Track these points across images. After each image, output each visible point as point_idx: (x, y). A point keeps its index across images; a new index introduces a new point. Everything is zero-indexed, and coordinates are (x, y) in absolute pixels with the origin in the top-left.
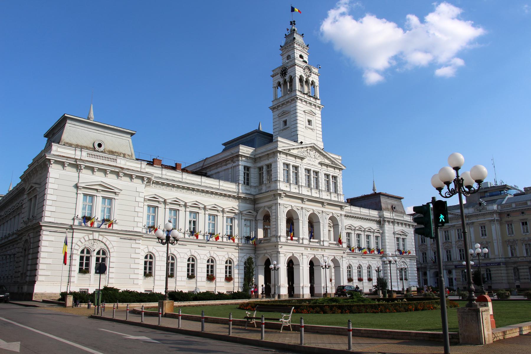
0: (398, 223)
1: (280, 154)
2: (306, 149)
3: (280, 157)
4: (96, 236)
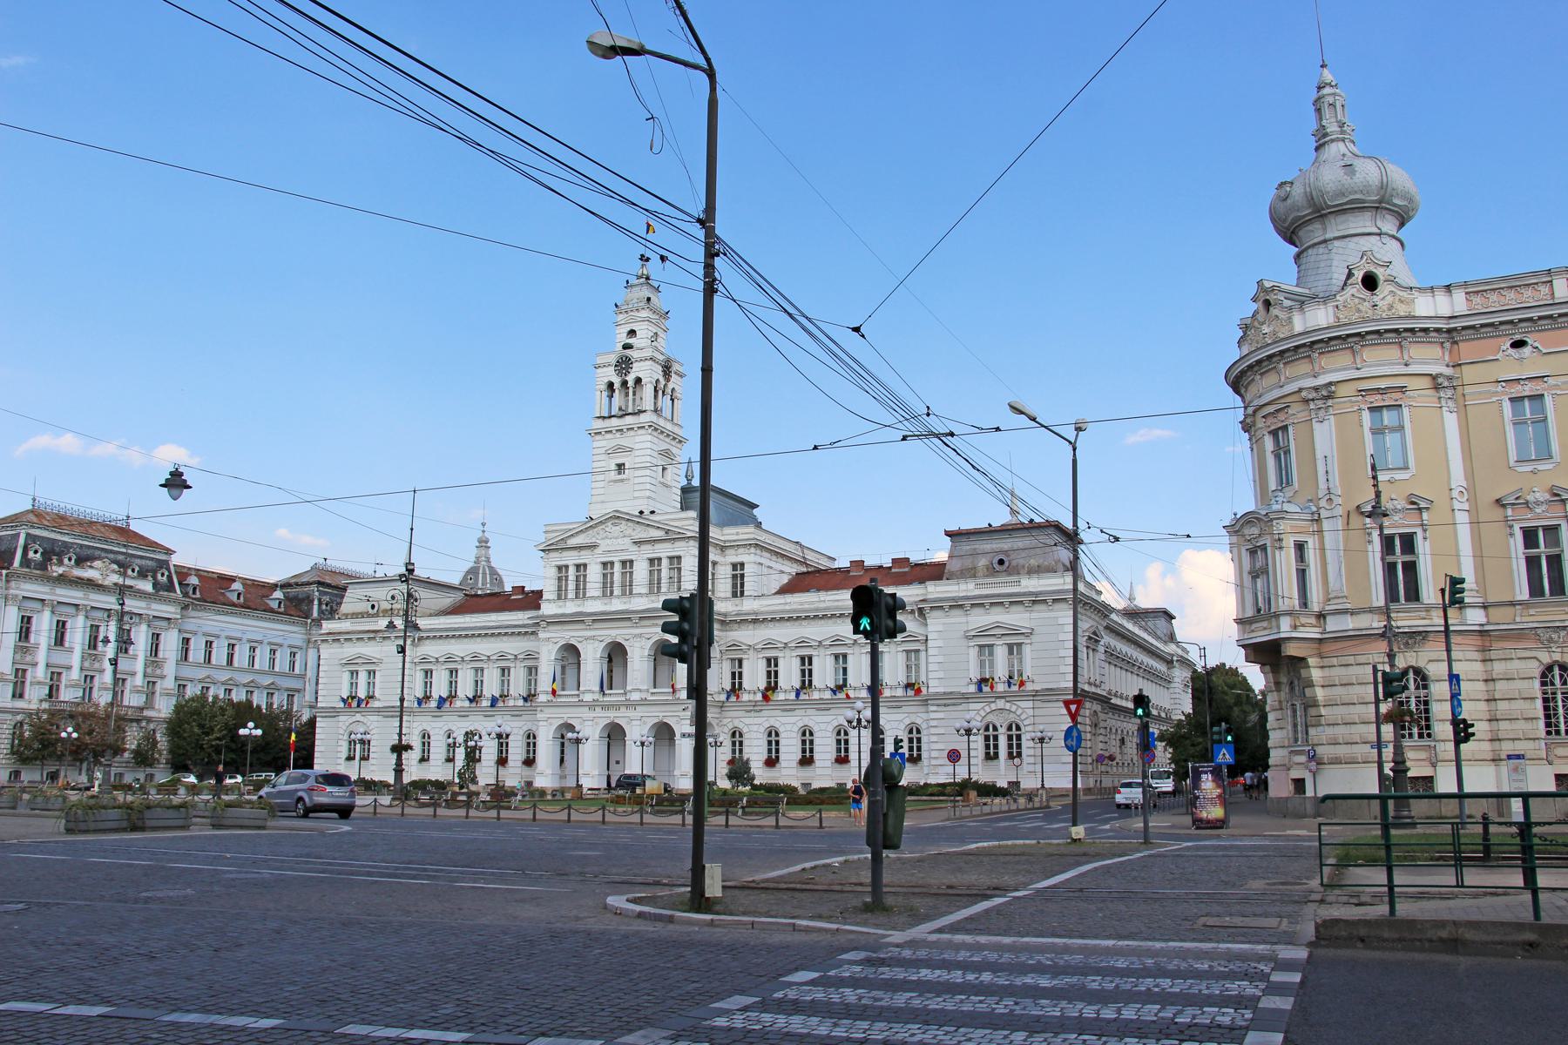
2: (603, 527)
4: (358, 717)
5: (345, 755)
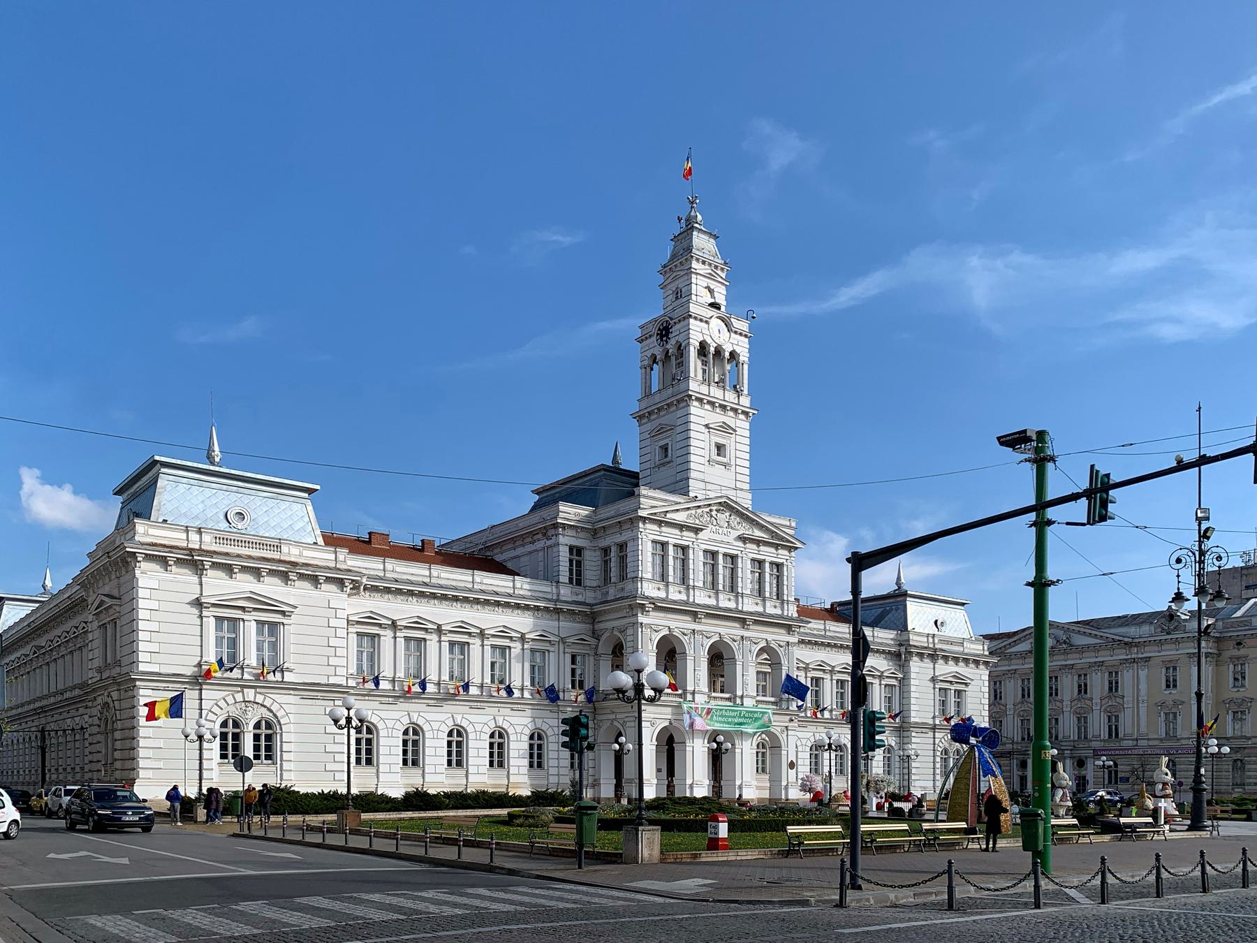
0: (946, 658)
1: (644, 523)
2: (708, 510)
3: (645, 529)
4: (250, 694)
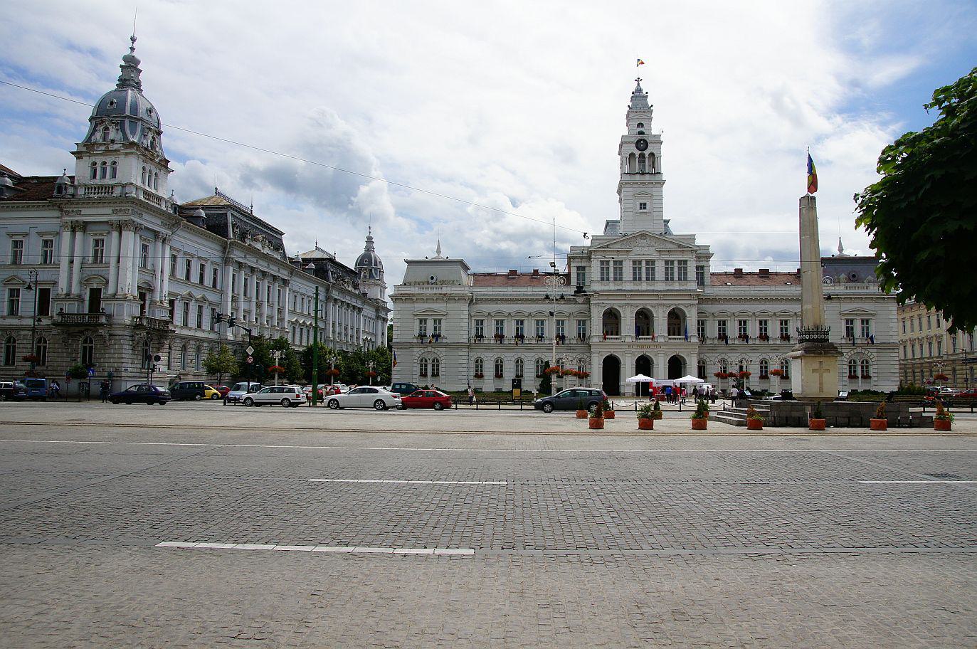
4: (429, 349)
5: (418, 373)
